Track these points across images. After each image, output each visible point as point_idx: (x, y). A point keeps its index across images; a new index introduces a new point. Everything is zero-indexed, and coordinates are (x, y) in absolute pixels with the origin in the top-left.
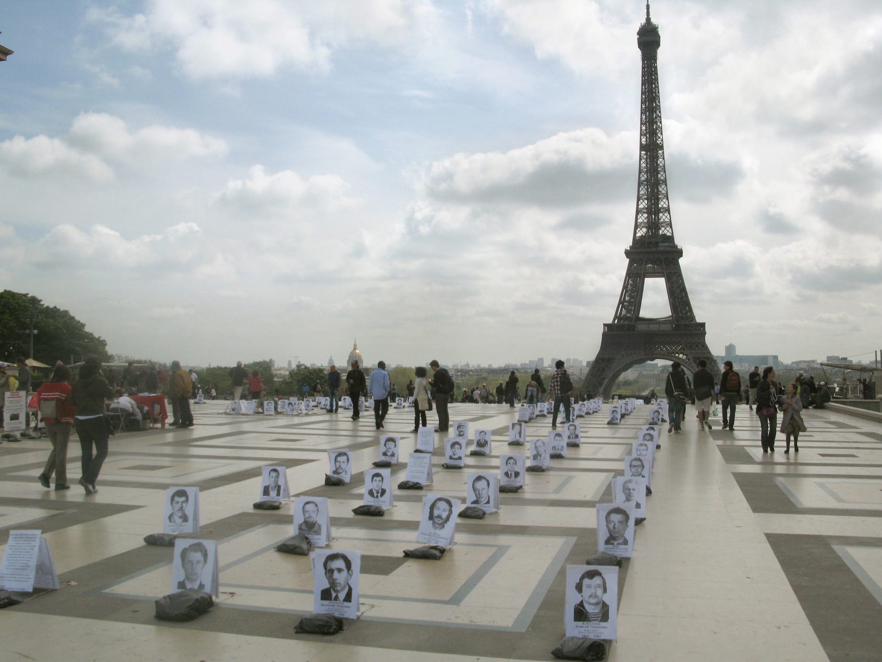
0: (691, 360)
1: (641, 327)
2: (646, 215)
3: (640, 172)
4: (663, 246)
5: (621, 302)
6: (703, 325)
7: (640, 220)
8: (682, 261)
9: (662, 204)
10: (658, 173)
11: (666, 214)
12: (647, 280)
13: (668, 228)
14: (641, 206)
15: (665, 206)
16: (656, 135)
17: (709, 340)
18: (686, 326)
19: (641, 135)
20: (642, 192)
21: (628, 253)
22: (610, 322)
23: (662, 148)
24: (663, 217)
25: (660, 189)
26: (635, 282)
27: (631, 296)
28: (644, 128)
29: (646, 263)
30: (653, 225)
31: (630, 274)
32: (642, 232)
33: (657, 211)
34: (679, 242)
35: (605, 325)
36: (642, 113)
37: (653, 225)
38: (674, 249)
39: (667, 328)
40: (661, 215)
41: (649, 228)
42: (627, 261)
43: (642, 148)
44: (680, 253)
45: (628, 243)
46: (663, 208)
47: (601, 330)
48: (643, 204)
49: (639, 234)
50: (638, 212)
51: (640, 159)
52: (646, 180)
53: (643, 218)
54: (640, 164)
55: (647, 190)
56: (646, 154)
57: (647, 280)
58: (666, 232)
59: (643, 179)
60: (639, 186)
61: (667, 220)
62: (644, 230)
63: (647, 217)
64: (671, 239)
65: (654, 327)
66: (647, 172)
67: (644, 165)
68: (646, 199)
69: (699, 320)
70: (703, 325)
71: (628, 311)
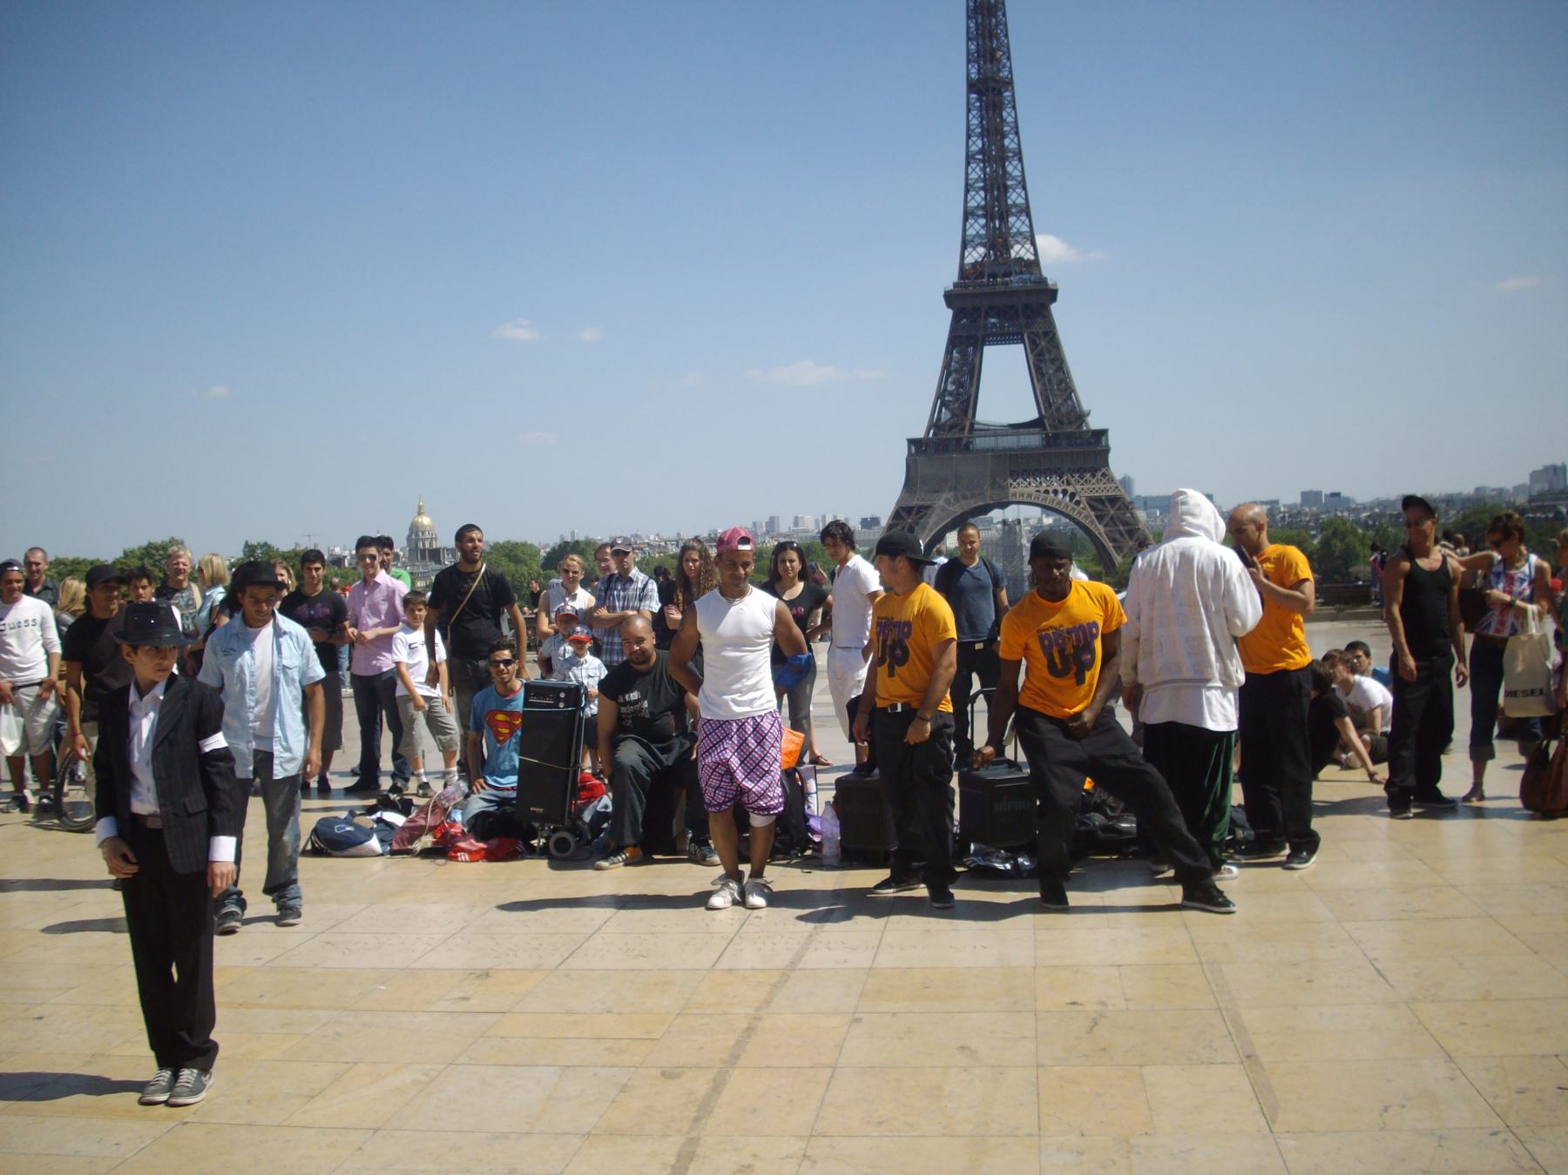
0: (1084, 504)
1: (980, 443)
2: (983, 221)
3: (969, 137)
4: (1015, 281)
5: (941, 395)
6: (1104, 432)
7: (971, 232)
8: (1054, 308)
9: (1015, 197)
10: (1004, 136)
11: (1023, 218)
12: (987, 349)
13: (1028, 246)
14: (972, 204)
15: (1020, 201)
16: (999, 60)
17: (1119, 464)
18: (1069, 436)
19: (969, 61)
20: (973, 176)
21: (950, 298)
22: (920, 433)
23: (1009, 83)
24: (1017, 224)
25: (1010, 168)
26: (963, 354)
27: (958, 384)
28: (973, 47)
29: (987, 315)
30: (998, 242)
31: (955, 341)
32: (976, 255)
33: (1003, 217)
34: (1046, 271)
35: (911, 442)
36: (969, 17)
37: (998, 242)
38: (1042, 287)
39: (1033, 440)
40: (1012, 219)
41: (991, 245)
42: (948, 314)
43: (972, 86)
44: (1052, 295)
45: (950, 277)
46: (1015, 205)
47: (903, 451)
48: (978, 199)
49: (969, 260)
50: (968, 214)
51: (969, 110)
52: (982, 151)
53: (977, 227)
54: (968, 121)
55: (983, 170)
56: (979, 100)
57: (987, 349)
58: (1022, 253)
59: (974, 148)
60: (968, 164)
61: (1025, 229)
62: (982, 250)
63: (986, 226)
64: (1035, 264)
65: (1008, 442)
66: (981, 135)
67: (975, 122)
68: (983, 188)
69: (1094, 423)
70: (1104, 432)
71: (954, 415)
